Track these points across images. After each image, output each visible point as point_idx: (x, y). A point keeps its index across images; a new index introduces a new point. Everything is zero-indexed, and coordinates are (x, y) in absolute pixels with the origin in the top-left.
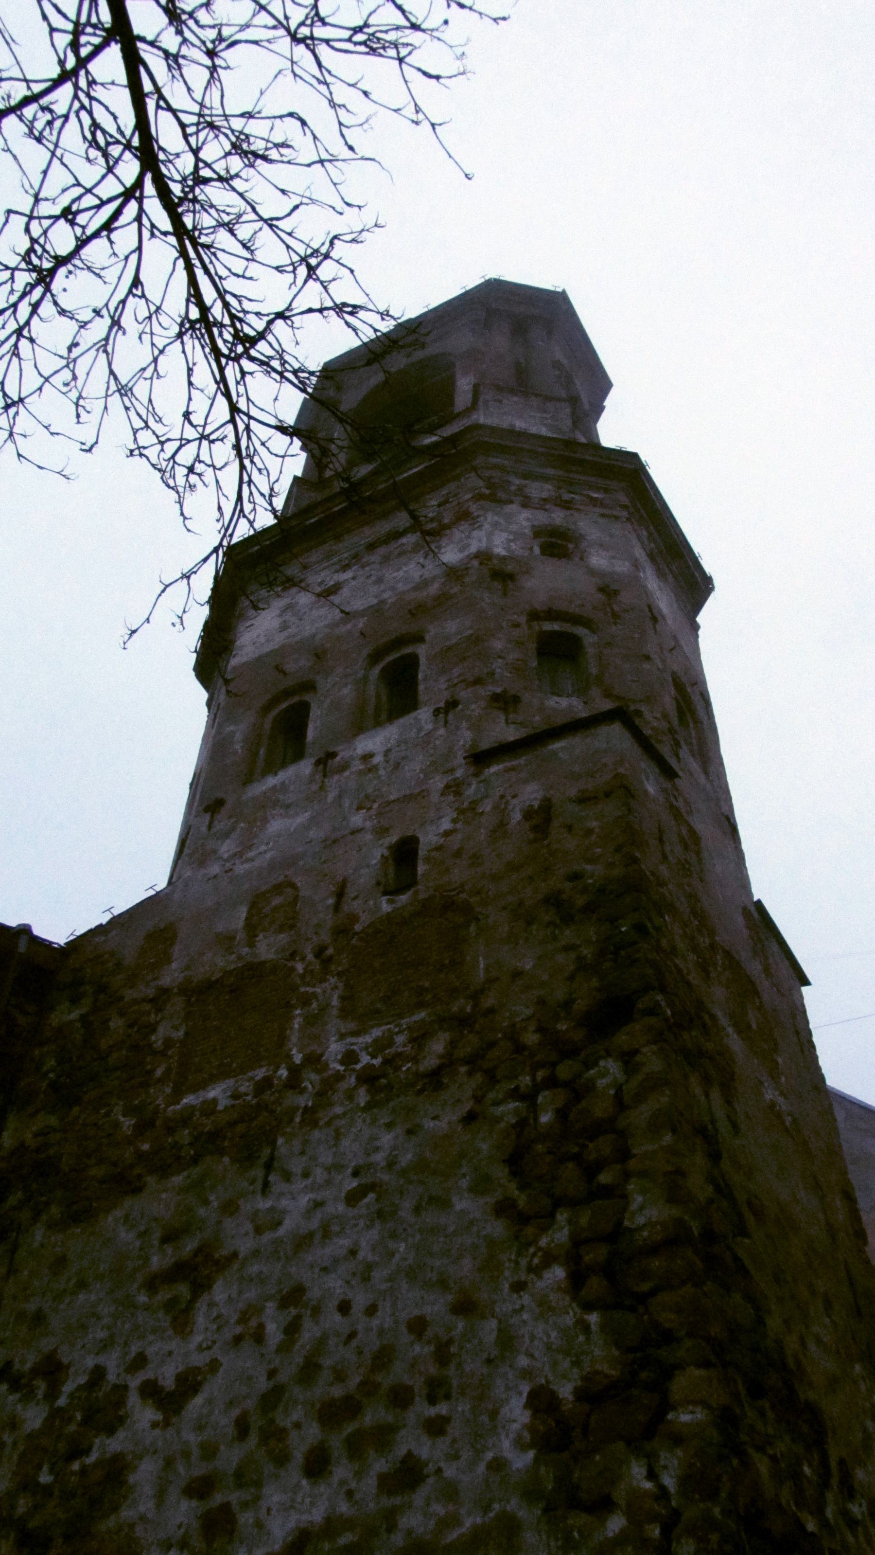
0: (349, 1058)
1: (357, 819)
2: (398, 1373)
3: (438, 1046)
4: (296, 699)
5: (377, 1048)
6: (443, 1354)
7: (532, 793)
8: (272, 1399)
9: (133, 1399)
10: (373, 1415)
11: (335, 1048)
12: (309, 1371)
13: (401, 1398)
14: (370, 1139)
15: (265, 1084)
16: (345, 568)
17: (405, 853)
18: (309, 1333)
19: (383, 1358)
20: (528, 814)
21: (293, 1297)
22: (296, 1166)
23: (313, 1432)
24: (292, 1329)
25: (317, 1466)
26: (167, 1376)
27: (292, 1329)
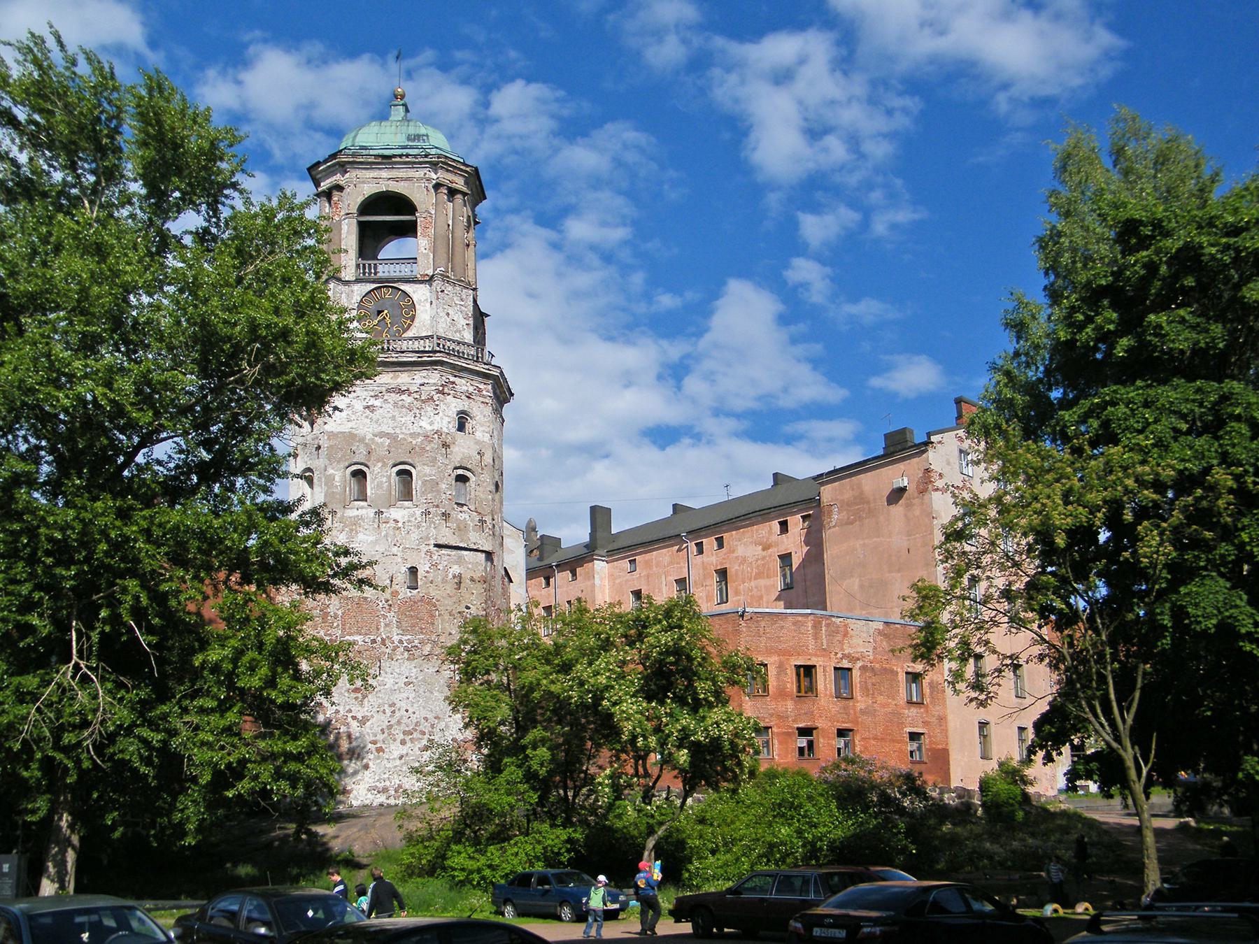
0: (401, 642)
1: (395, 550)
2: (421, 728)
3: (427, 648)
4: (359, 467)
5: (409, 641)
6: (432, 726)
7: (456, 569)
8: (390, 727)
9: (350, 719)
10: (415, 735)
11: (396, 638)
12: (399, 723)
13: (423, 733)
14: (408, 669)
15: (374, 641)
17: (413, 571)
18: (397, 714)
19: (417, 724)
20: (454, 577)
21: (393, 705)
22: (388, 670)
23: (401, 736)
24: (393, 712)
25: (403, 742)
26: (359, 716)
27: (393, 712)
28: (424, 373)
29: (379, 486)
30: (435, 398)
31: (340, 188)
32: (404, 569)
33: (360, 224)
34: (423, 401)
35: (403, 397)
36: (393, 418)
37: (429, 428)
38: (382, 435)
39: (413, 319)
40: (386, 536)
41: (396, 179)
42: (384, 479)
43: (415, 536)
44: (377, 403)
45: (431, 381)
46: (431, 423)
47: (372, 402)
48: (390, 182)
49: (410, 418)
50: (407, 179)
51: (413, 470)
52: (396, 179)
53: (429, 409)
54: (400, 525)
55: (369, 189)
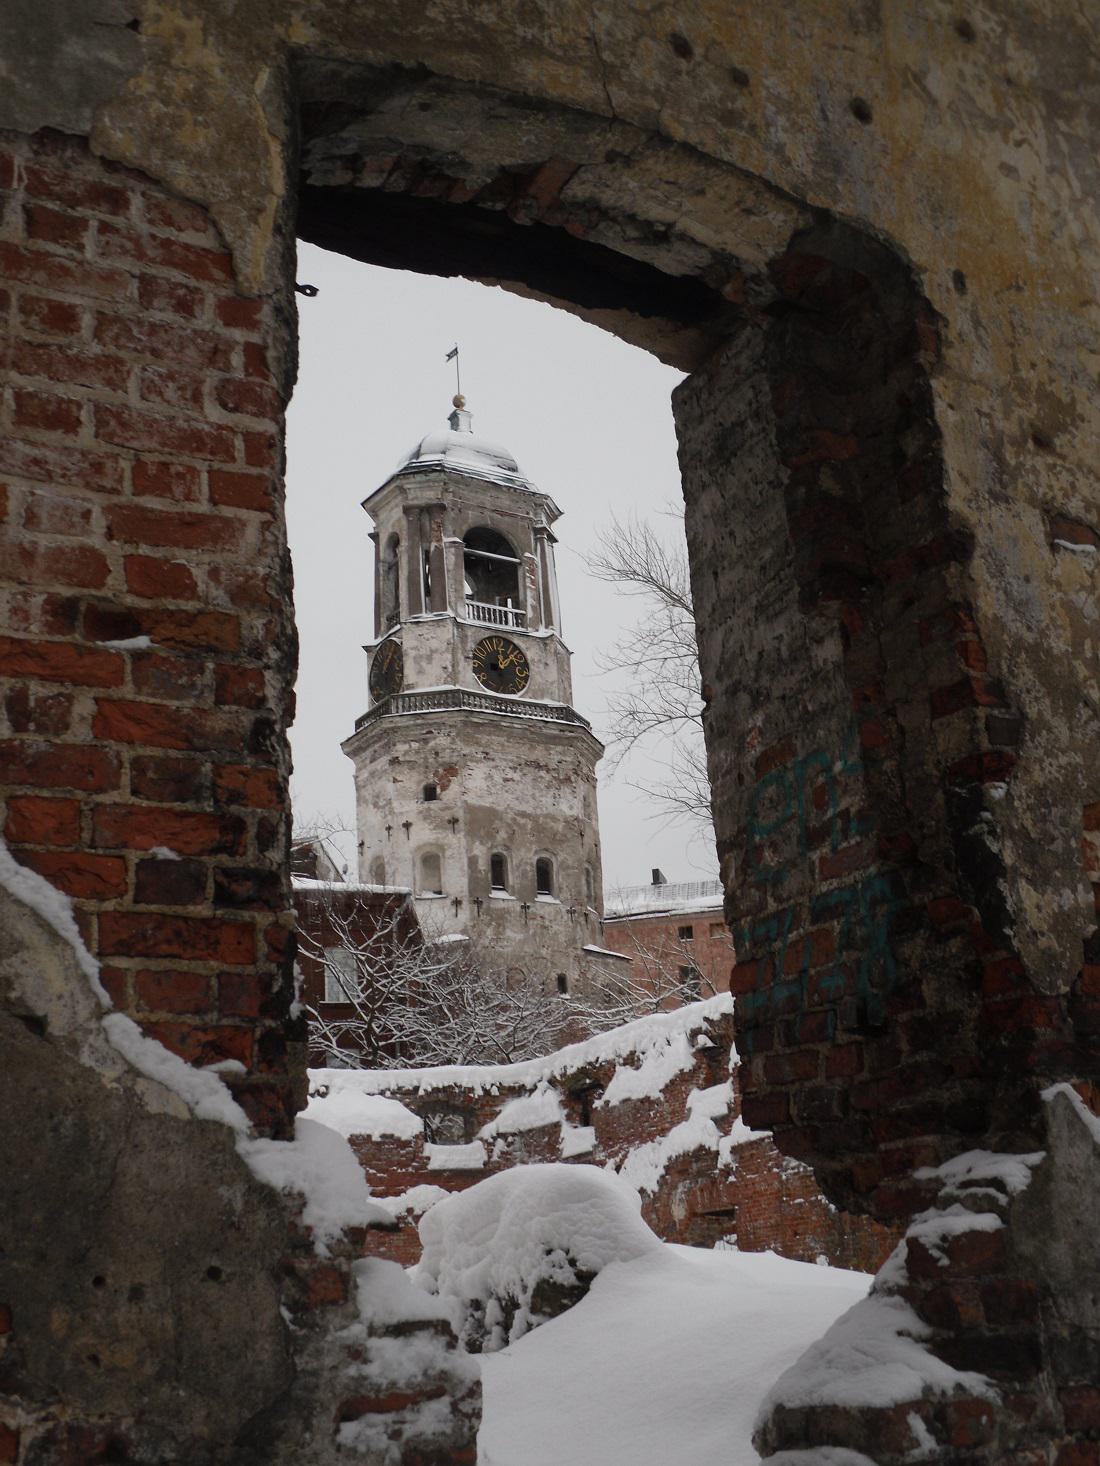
16: (514, 769)
28: (559, 748)
29: (524, 874)
30: (573, 779)
31: (443, 508)
32: (554, 976)
33: (467, 556)
34: (562, 782)
35: (543, 773)
36: (533, 797)
37: (569, 813)
38: (523, 815)
39: (526, 678)
40: (534, 935)
41: (503, 514)
42: (528, 868)
43: (562, 938)
44: (516, 776)
45: (568, 759)
46: (571, 808)
47: (510, 774)
48: (495, 515)
49: (547, 800)
50: (511, 515)
51: (553, 860)
52: (503, 514)
53: (566, 790)
54: (547, 923)
55: (472, 518)
